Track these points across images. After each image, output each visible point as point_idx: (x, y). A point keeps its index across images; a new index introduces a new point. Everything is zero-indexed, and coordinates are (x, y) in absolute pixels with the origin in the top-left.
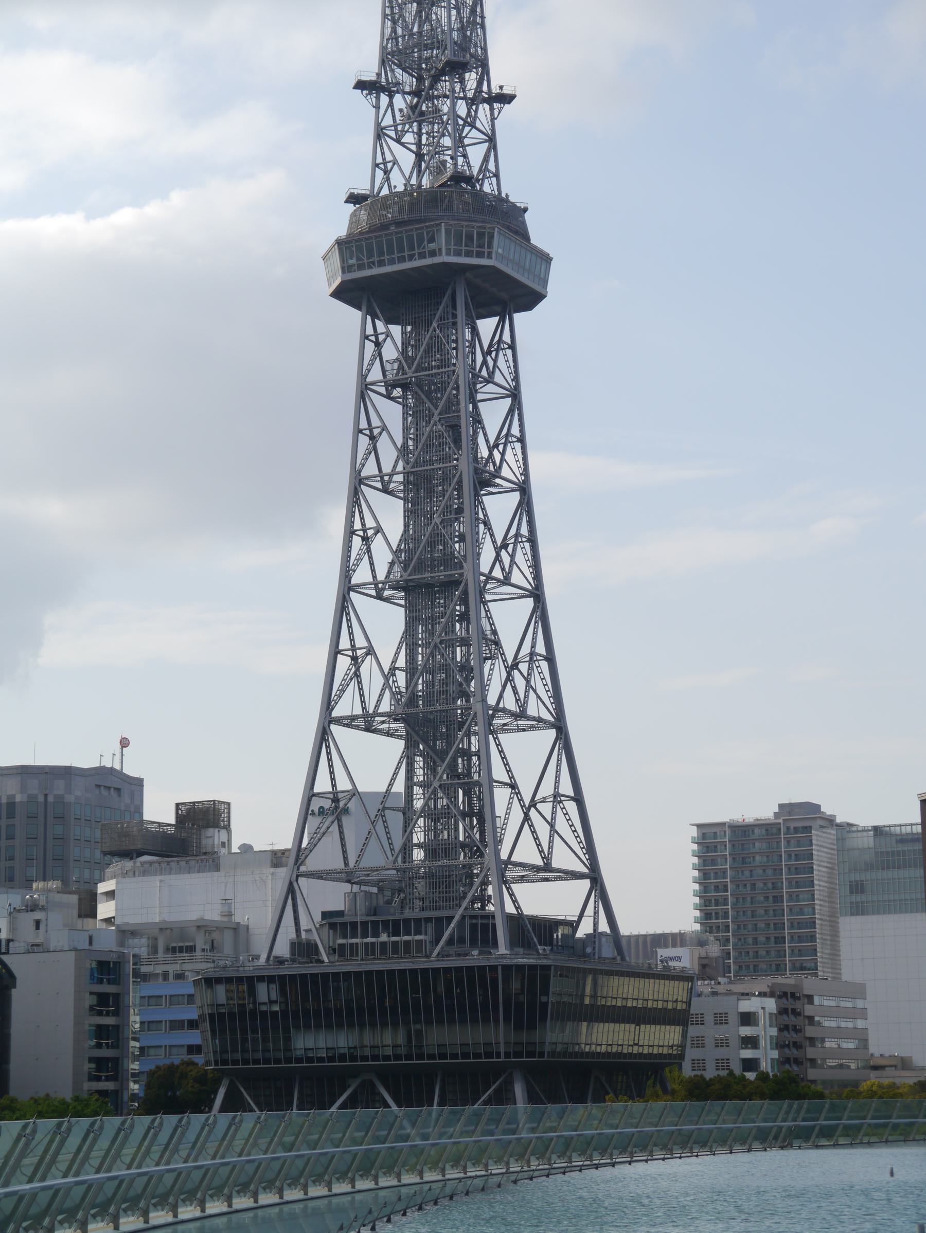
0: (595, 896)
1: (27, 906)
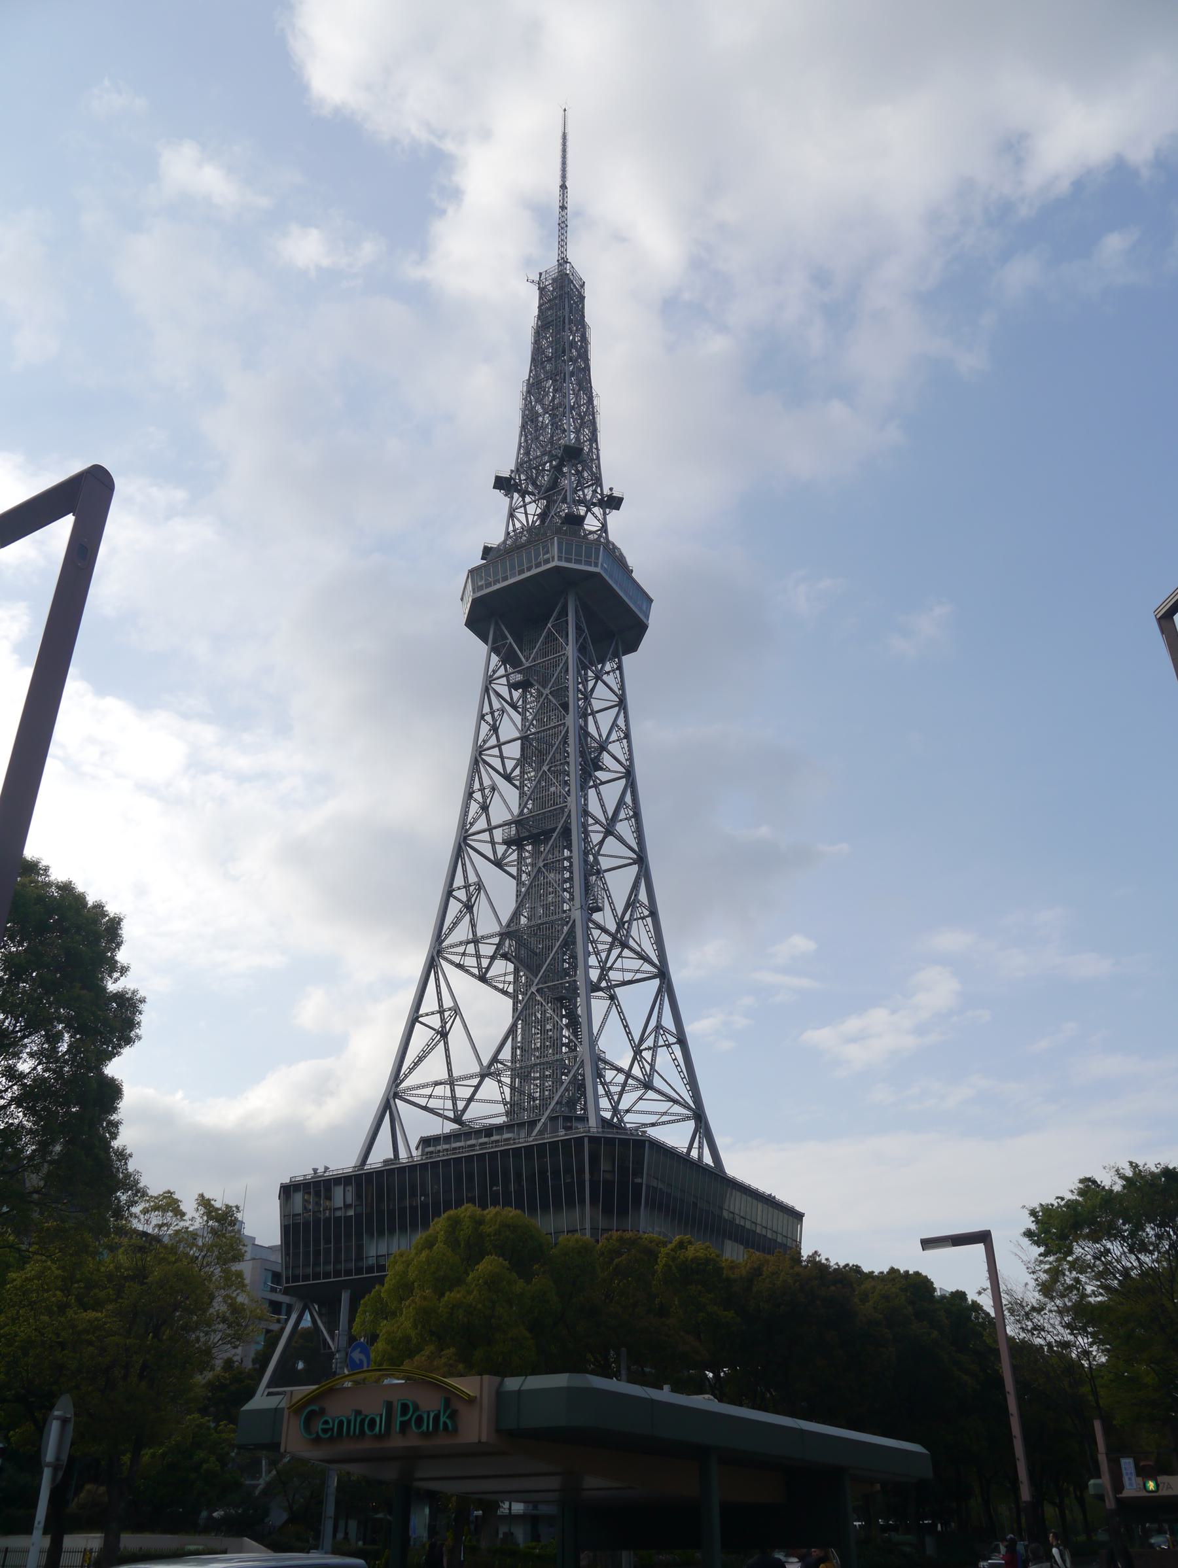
0: (700, 1137)
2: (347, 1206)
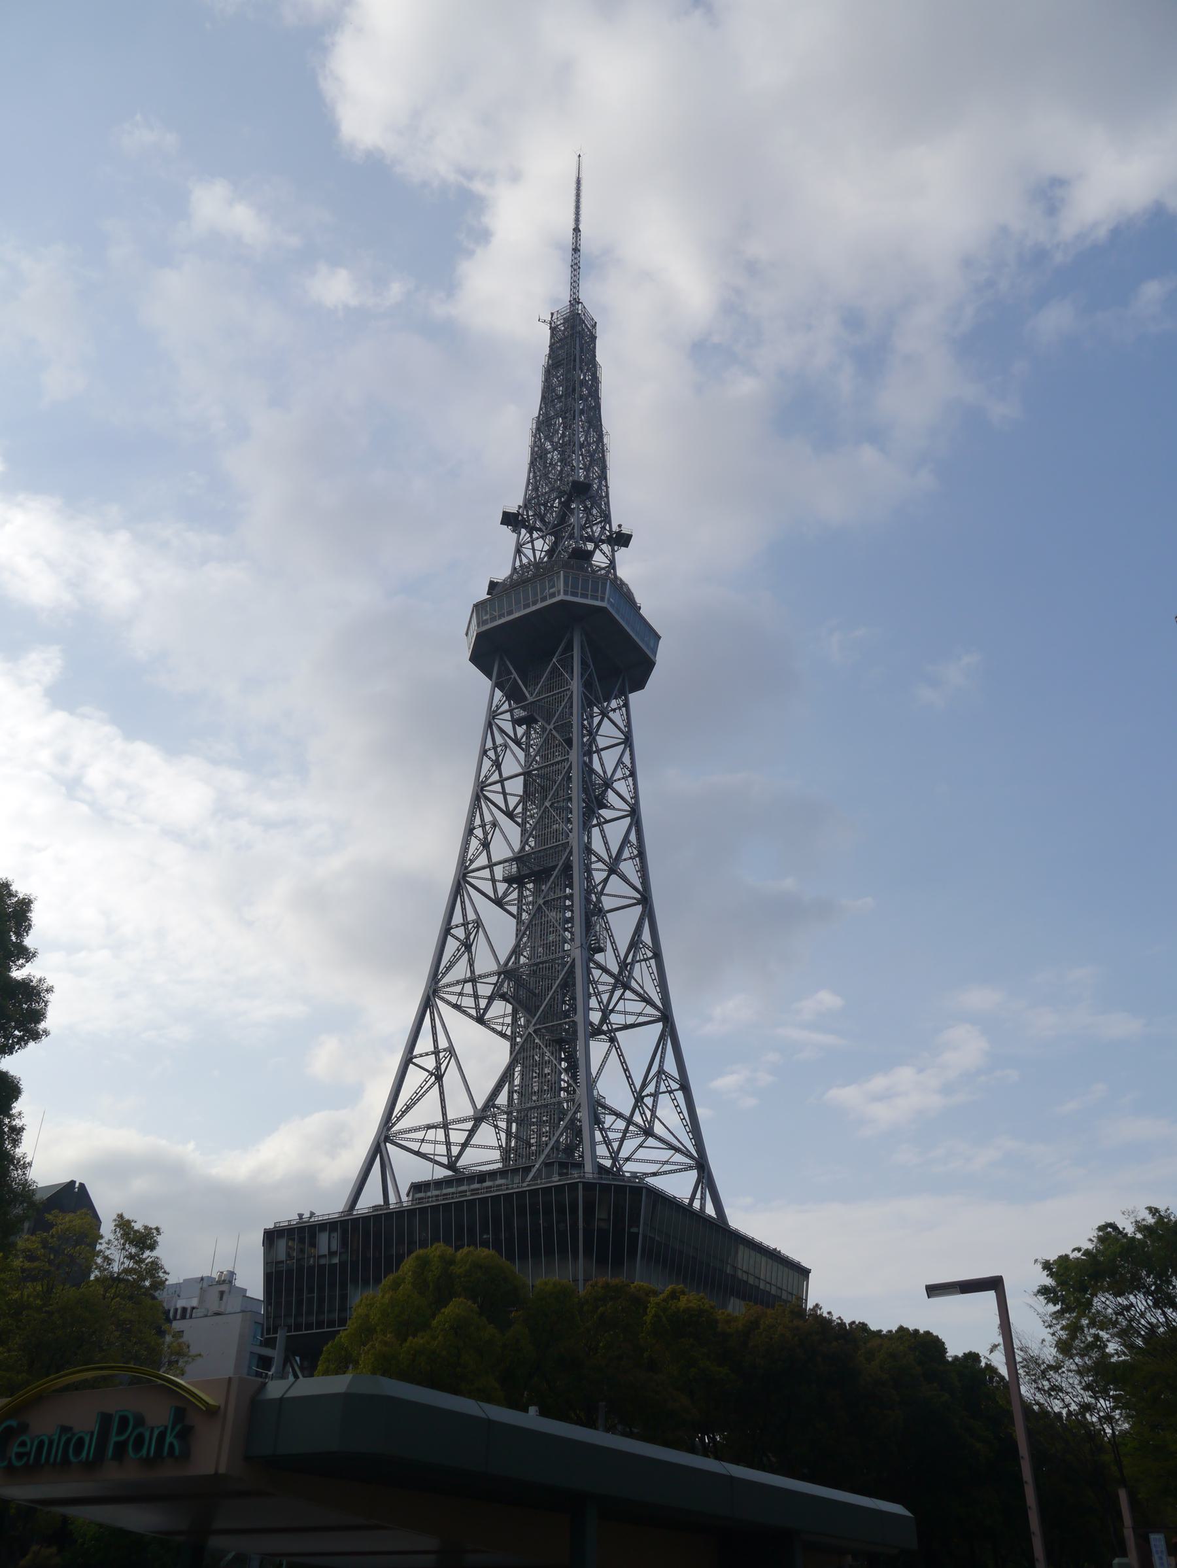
0: (702, 1186)
2: (332, 1254)
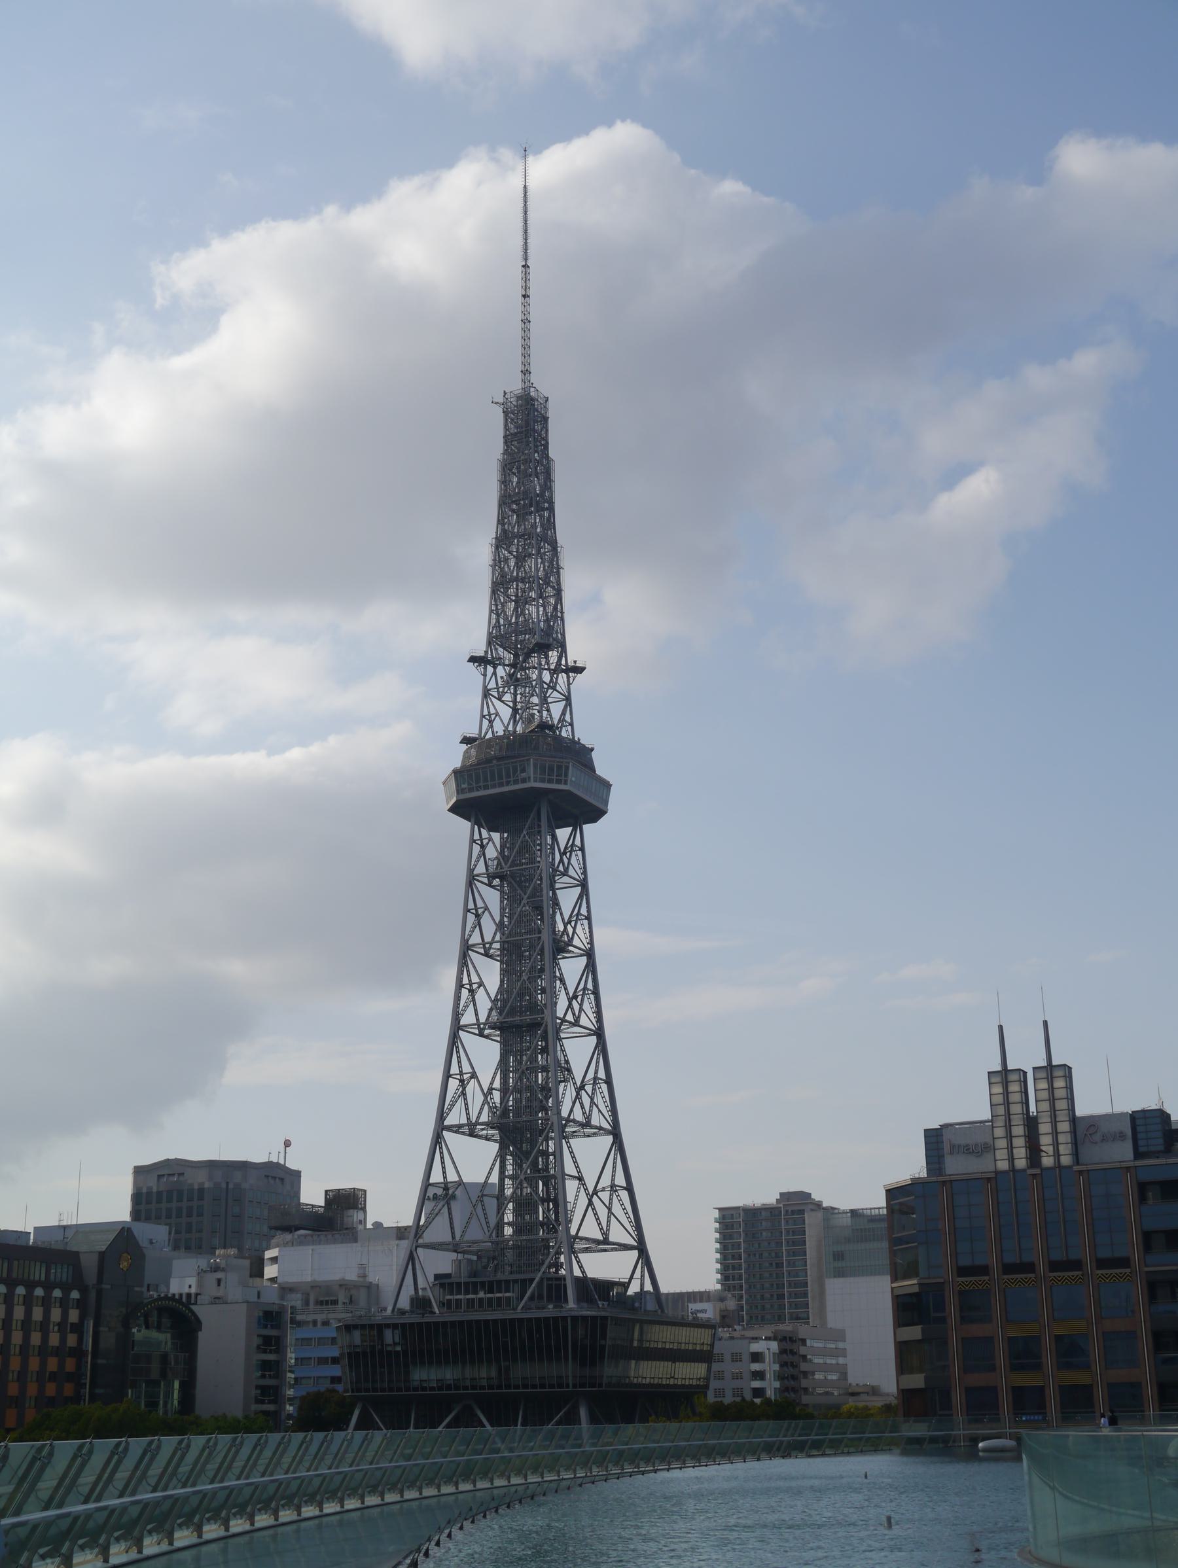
0: (642, 1263)
1: (211, 1268)
2: (395, 1344)
